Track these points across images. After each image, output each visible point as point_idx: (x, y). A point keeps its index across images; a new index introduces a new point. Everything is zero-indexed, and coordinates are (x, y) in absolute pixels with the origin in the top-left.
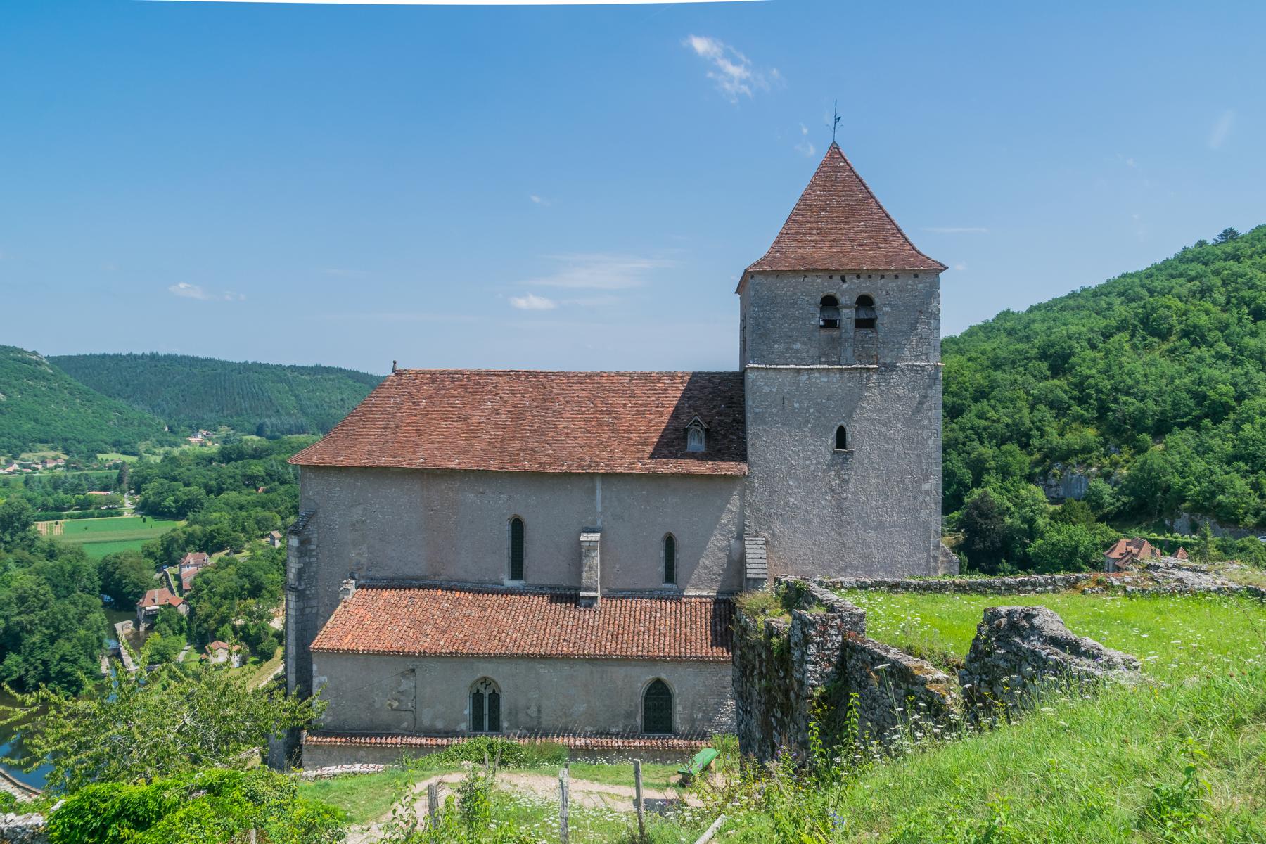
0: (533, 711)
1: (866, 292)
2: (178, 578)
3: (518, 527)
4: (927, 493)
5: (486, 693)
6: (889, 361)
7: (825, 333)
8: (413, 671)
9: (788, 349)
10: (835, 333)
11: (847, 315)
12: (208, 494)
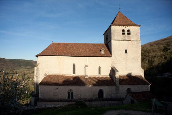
1: (129, 29)
4: (139, 60)
5: (71, 92)
7: (123, 35)
8: (57, 88)
9: (117, 37)
10: (124, 35)
11: (126, 33)
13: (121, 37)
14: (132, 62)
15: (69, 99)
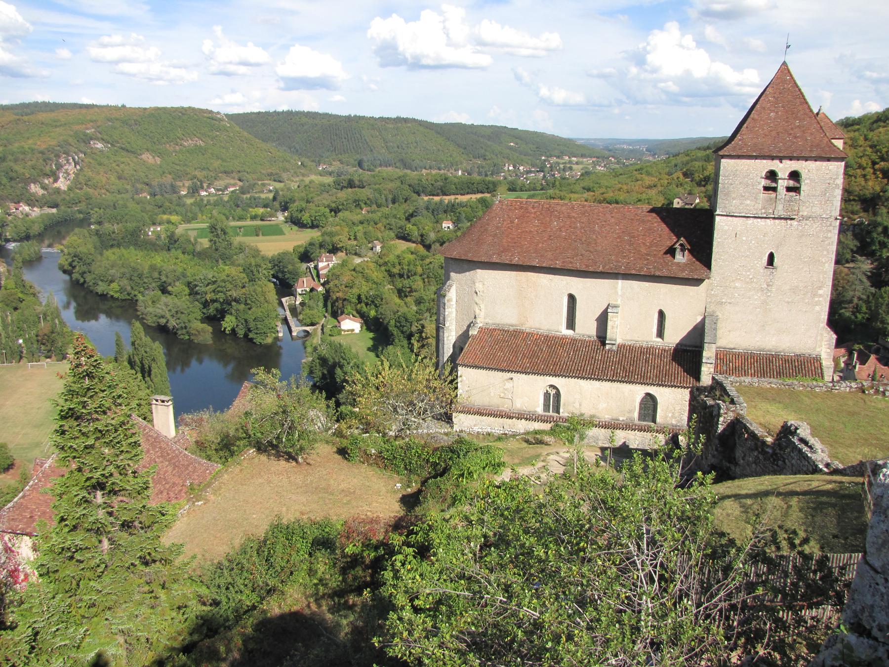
0: (577, 405)
2: (316, 267)
3: (572, 299)
4: (821, 296)
6: (805, 214)
9: (741, 204)
10: (773, 195)
11: (782, 184)
12: (331, 212)
13: (758, 201)
14: (788, 303)
15: (547, 414)
